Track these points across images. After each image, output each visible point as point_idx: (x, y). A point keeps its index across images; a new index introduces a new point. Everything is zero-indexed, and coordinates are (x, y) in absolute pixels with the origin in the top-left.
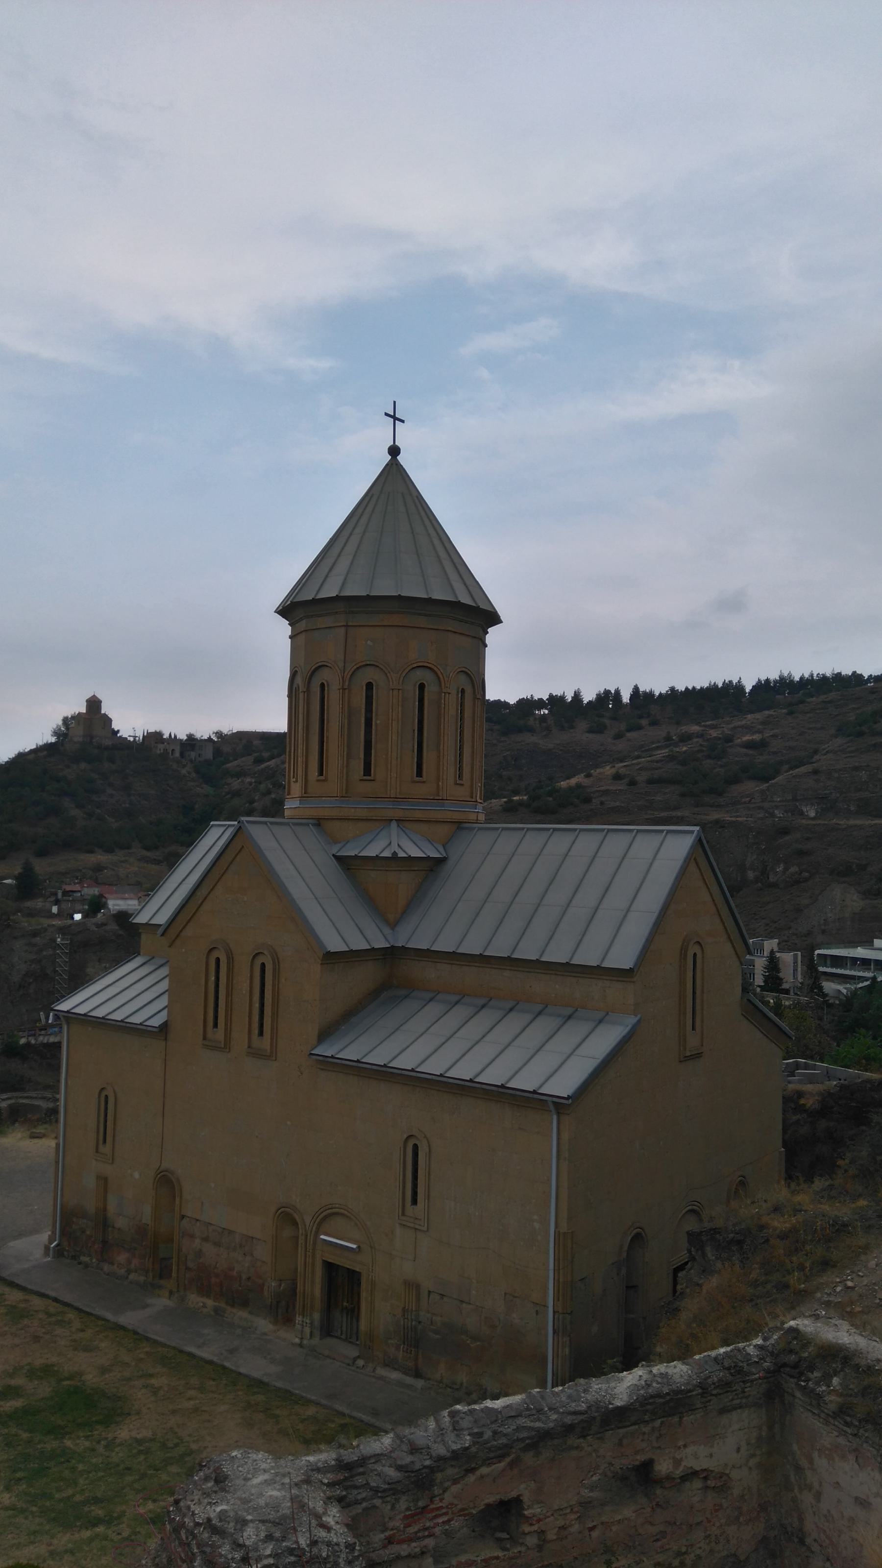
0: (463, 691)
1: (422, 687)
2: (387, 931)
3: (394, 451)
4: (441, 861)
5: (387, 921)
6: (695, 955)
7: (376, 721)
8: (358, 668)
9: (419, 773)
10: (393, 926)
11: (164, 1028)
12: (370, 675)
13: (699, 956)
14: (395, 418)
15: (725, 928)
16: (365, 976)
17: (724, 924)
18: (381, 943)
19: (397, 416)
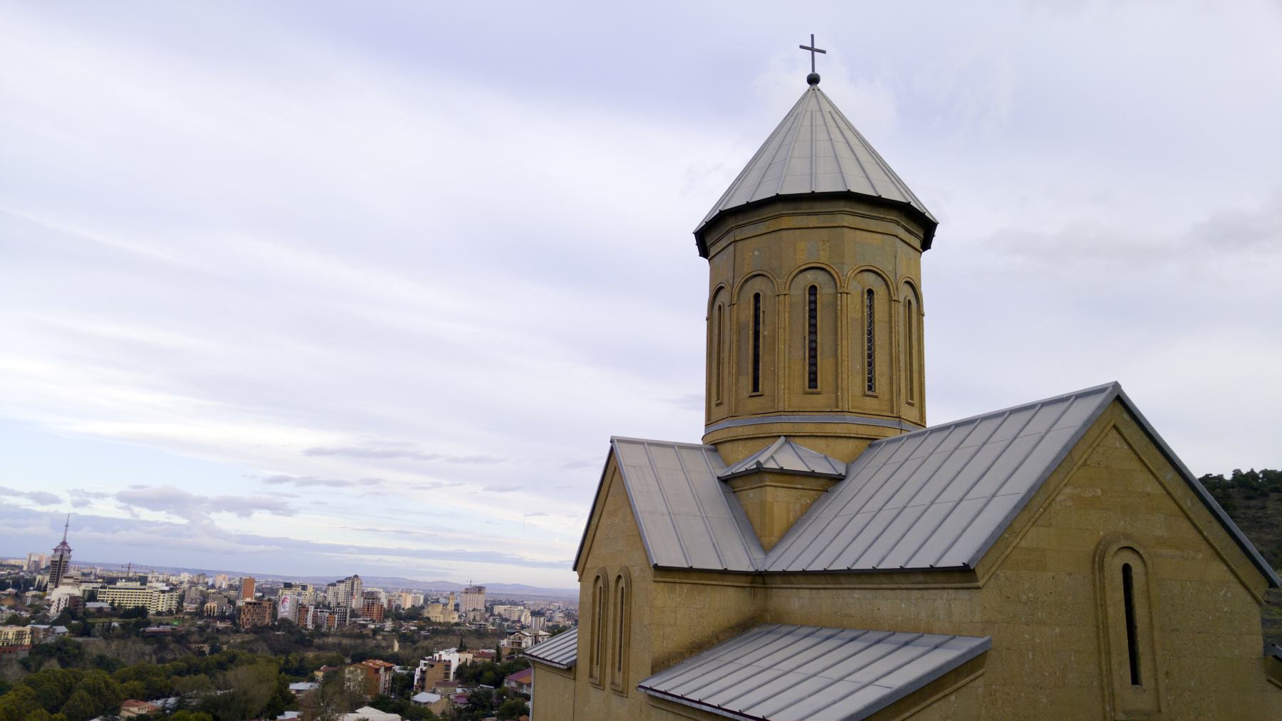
0: (870, 292)
1: (813, 290)
2: (758, 555)
3: (813, 80)
4: (838, 479)
5: (762, 546)
6: (1127, 569)
7: (764, 332)
8: (746, 281)
9: (813, 381)
10: (767, 549)
11: (571, 669)
12: (758, 285)
13: (1137, 570)
14: (812, 49)
15: (1205, 538)
16: (726, 604)
17: (1200, 532)
18: (745, 566)
19: (816, 47)
